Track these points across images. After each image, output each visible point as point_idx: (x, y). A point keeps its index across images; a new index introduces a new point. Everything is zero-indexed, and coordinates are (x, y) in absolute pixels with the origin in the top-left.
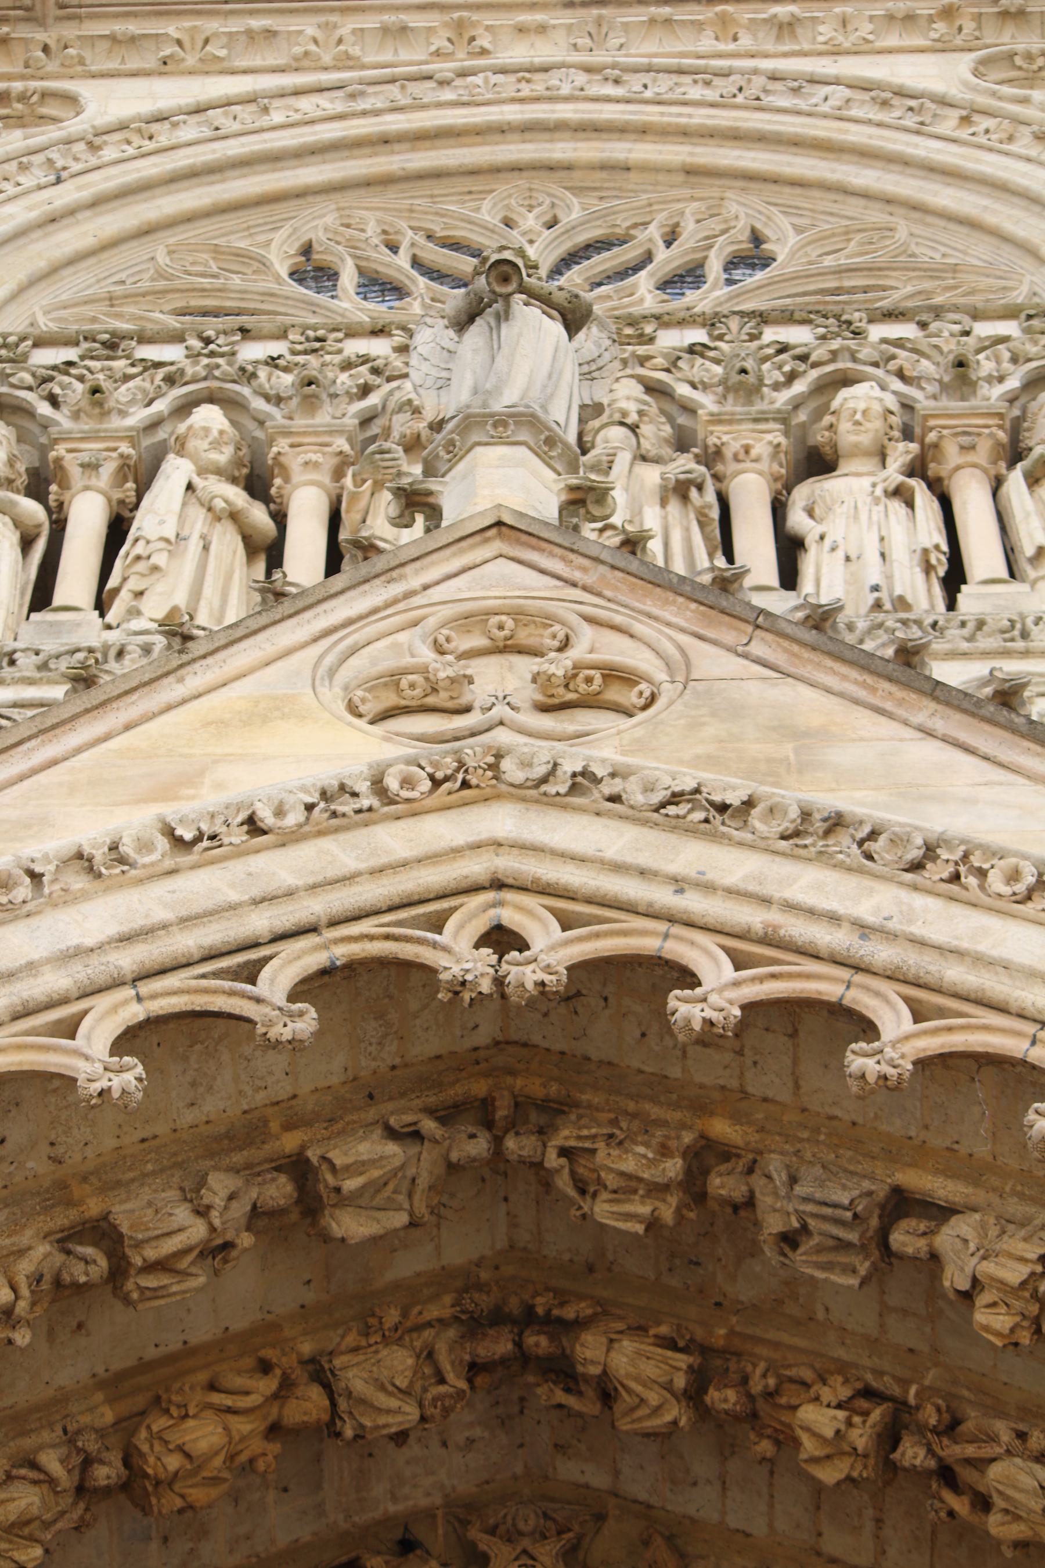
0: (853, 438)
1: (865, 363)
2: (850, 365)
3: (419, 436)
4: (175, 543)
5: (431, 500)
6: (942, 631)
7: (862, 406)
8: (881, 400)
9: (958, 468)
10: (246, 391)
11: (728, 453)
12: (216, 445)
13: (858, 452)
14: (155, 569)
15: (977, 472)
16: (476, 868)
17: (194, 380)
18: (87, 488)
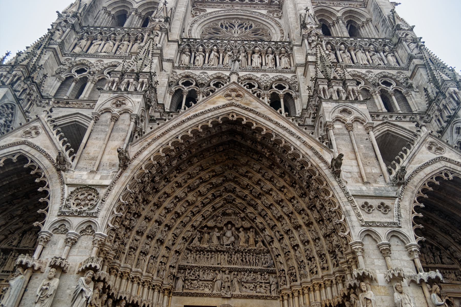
4: (213, 59)
16: (231, 111)
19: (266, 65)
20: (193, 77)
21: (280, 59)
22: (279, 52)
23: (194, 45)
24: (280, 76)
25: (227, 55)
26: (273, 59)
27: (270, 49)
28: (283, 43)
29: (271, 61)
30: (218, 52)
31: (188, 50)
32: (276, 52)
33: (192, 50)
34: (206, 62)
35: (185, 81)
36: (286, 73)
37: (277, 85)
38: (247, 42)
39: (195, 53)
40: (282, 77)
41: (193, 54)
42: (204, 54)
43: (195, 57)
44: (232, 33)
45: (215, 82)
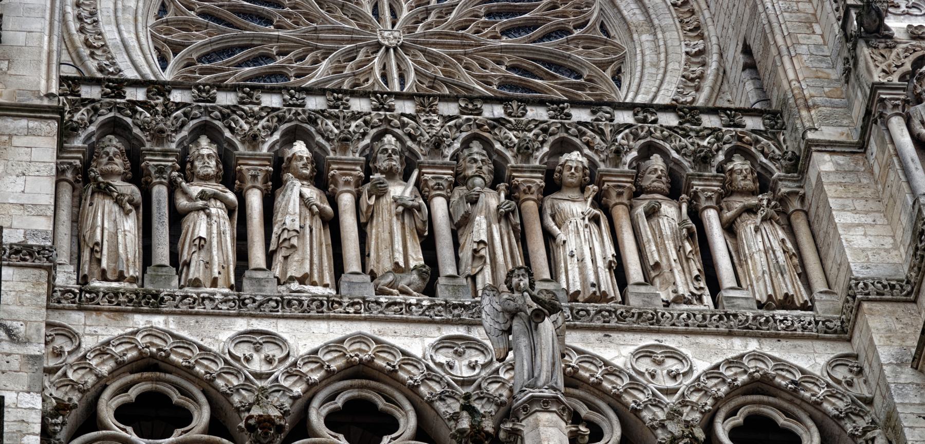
0: (570, 180)
1: (572, 135)
2: (565, 135)
3: (392, 167)
5: (519, 433)
6: (625, 317)
7: (574, 165)
8: (582, 162)
9: (616, 204)
10: (313, 130)
11: (522, 188)
12: (305, 166)
13: (571, 186)
14: (293, 246)
15: (624, 207)
17: (290, 120)
18: (254, 187)
19: (648, 281)
20: (188, 372)
21: (730, 229)
22: (716, 186)
23: (159, 136)
24: (757, 357)
25: (386, 201)
26: (690, 236)
27: (657, 162)
28: (732, 115)
29: (679, 249)
30: (320, 179)
31: (119, 165)
32: (697, 185)
33: (151, 162)
34: (257, 256)
35: (133, 393)
36: (789, 334)
37: (739, 419)
38: (498, 111)
39: (173, 188)
40: (769, 368)
41: (160, 192)
42: (231, 196)
43: (177, 218)
44: (357, 16)
45: (339, 402)
